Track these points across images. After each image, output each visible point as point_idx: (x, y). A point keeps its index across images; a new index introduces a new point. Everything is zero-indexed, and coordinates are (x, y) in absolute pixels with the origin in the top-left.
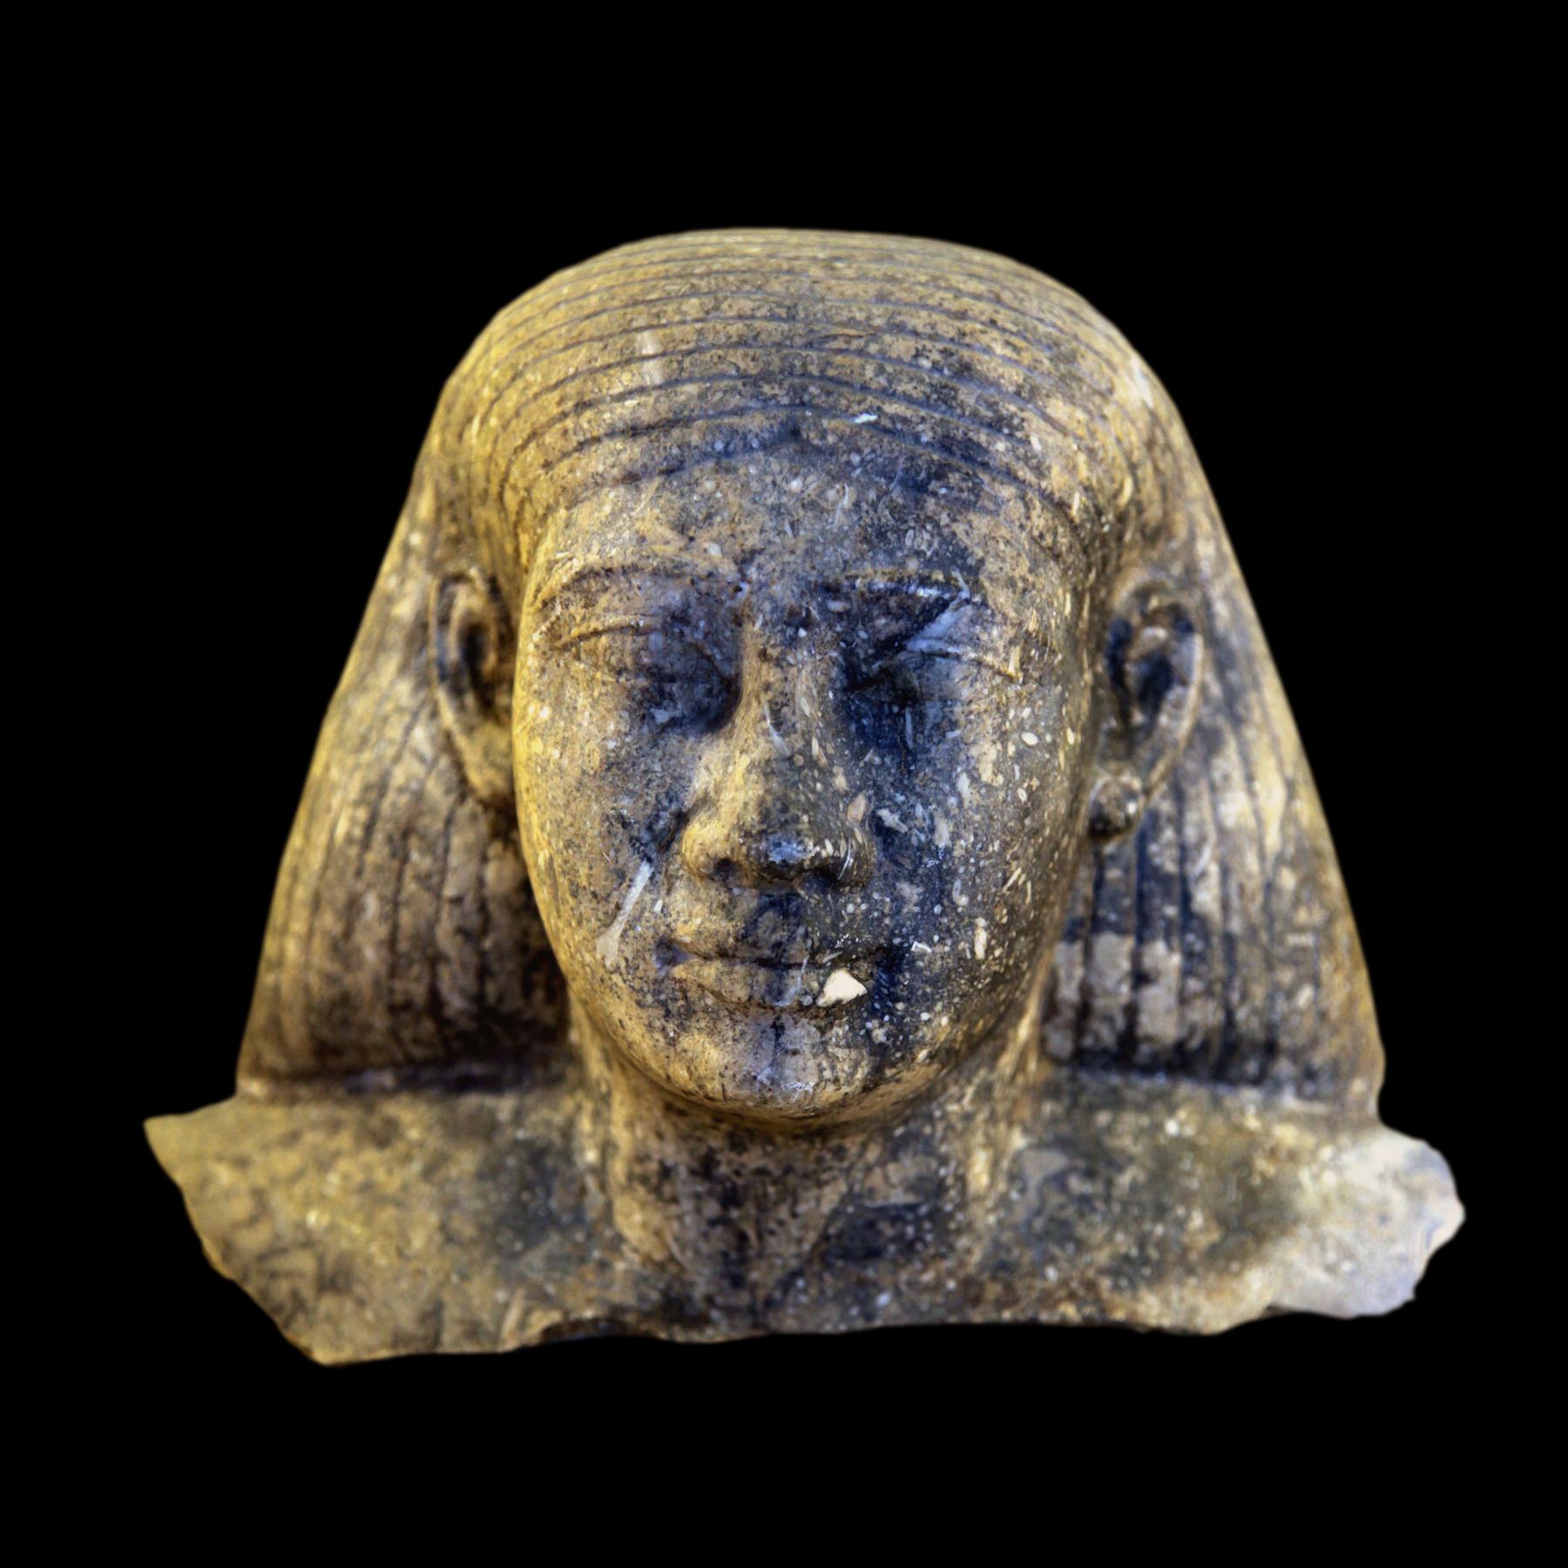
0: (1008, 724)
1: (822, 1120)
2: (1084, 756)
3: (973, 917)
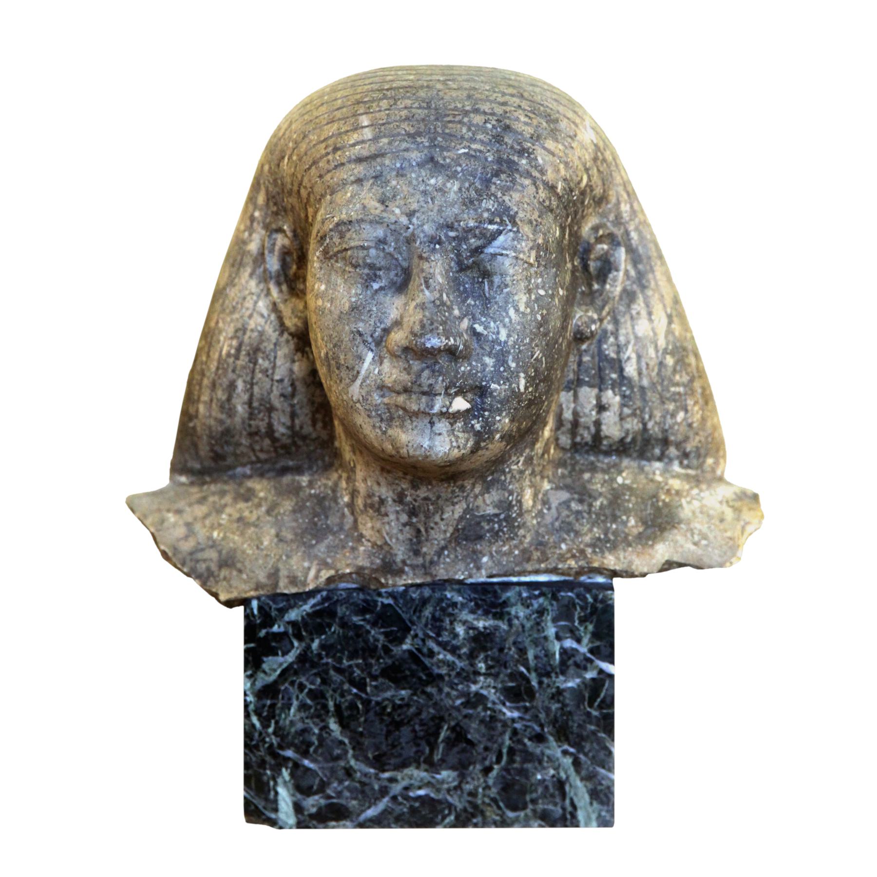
1: (453, 469)
2: (569, 302)
3: (518, 372)
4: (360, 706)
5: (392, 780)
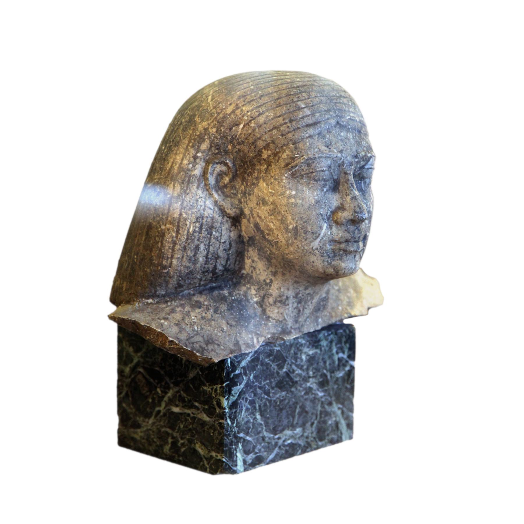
4: (268, 404)
5: (279, 438)
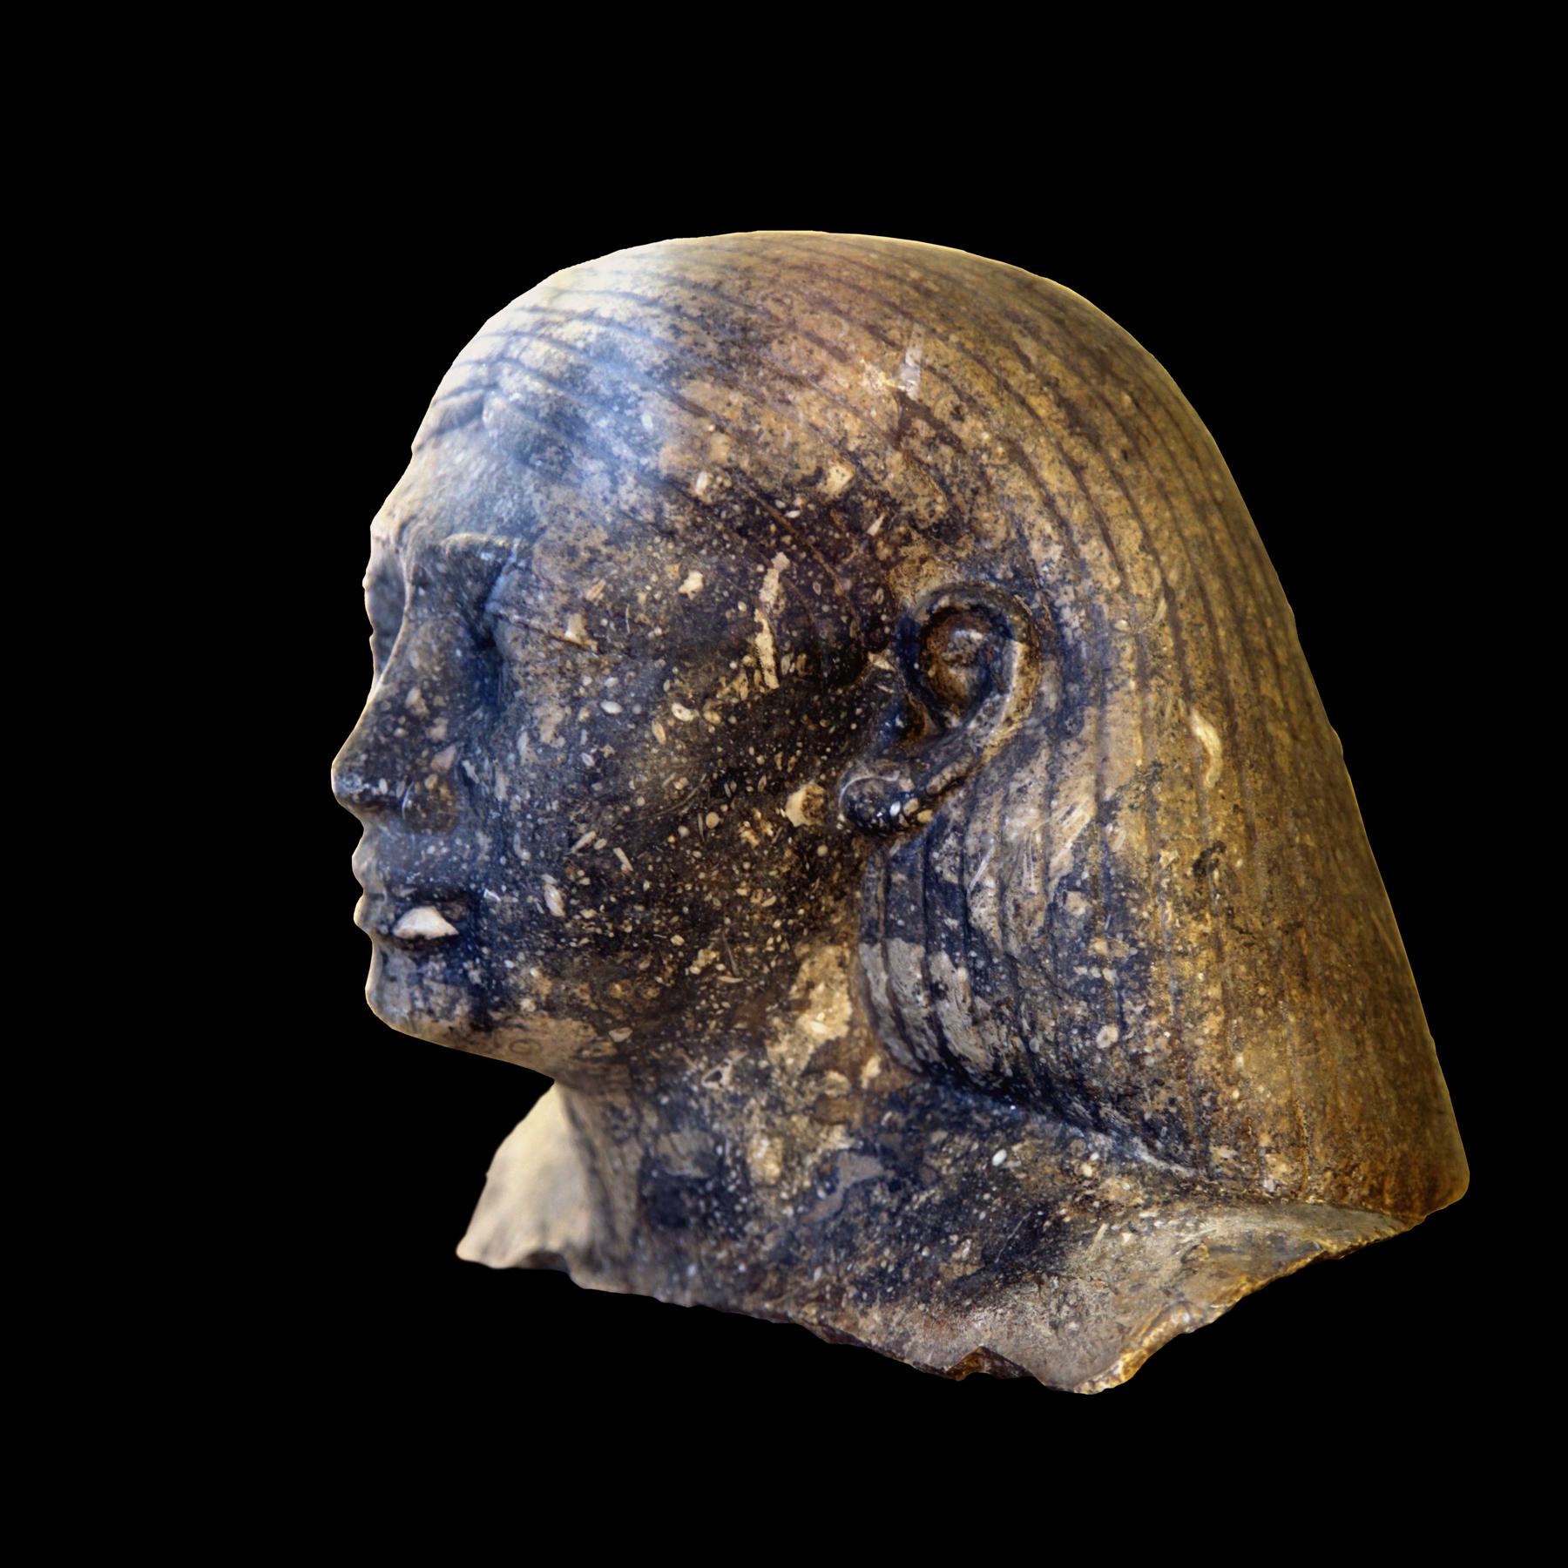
0: (582, 691)
